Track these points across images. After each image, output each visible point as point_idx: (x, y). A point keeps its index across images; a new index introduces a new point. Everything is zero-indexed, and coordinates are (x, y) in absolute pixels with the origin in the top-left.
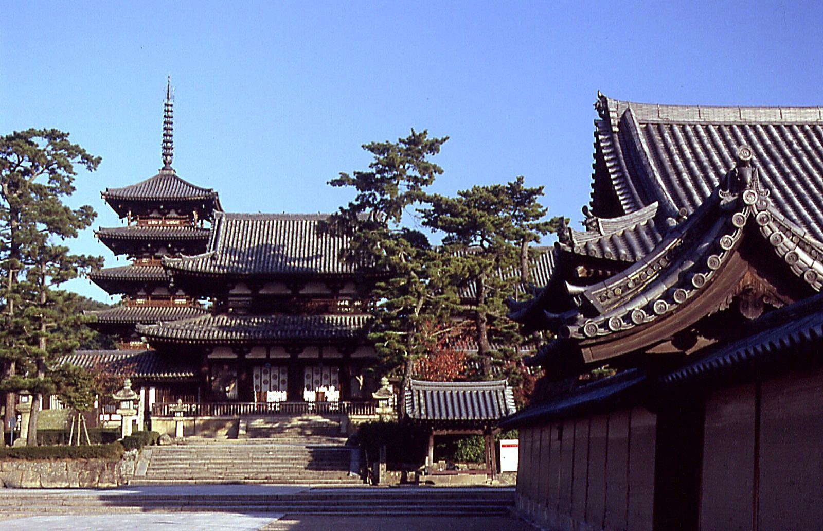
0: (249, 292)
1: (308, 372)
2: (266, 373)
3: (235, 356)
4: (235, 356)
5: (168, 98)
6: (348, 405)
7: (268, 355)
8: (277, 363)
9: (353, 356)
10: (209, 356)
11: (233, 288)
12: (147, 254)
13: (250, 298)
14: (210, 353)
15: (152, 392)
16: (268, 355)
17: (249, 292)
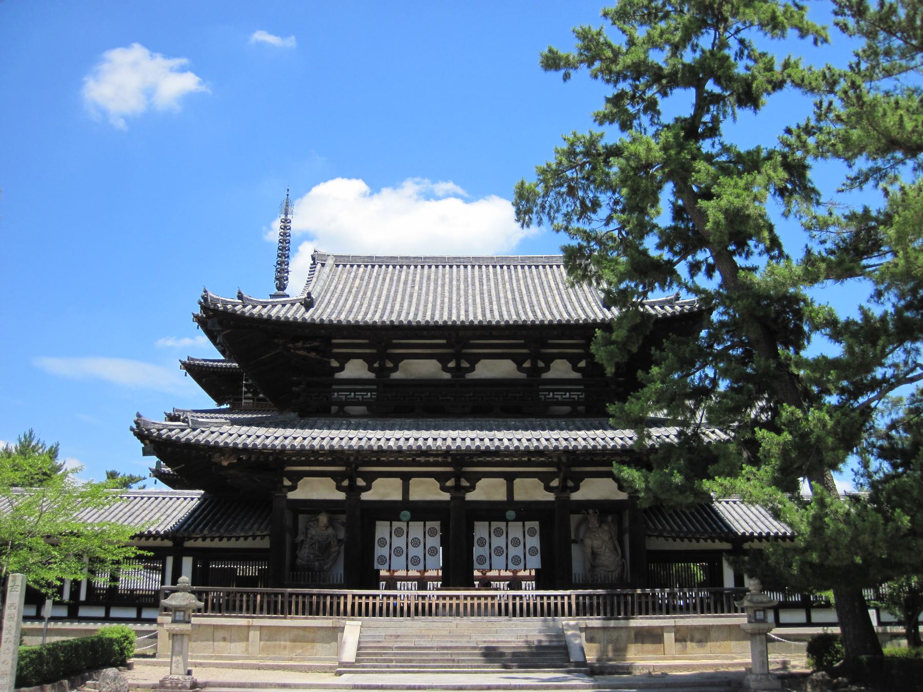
0: (371, 375)
1: (481, 530)
2: (399, 533)
3: (341, 496)
4: (341, 496)
5: (286, 214)
6: (577, 597)
7: (406, 491)
8: (422, 511)
9: (576, 496)
10: (291, 495)
11: (341, 368)
12: (250, 395)
13: (375, 387)
14: (293, 488)
15: (187, 563)
16: (406, 491)
17: (371, 375)
